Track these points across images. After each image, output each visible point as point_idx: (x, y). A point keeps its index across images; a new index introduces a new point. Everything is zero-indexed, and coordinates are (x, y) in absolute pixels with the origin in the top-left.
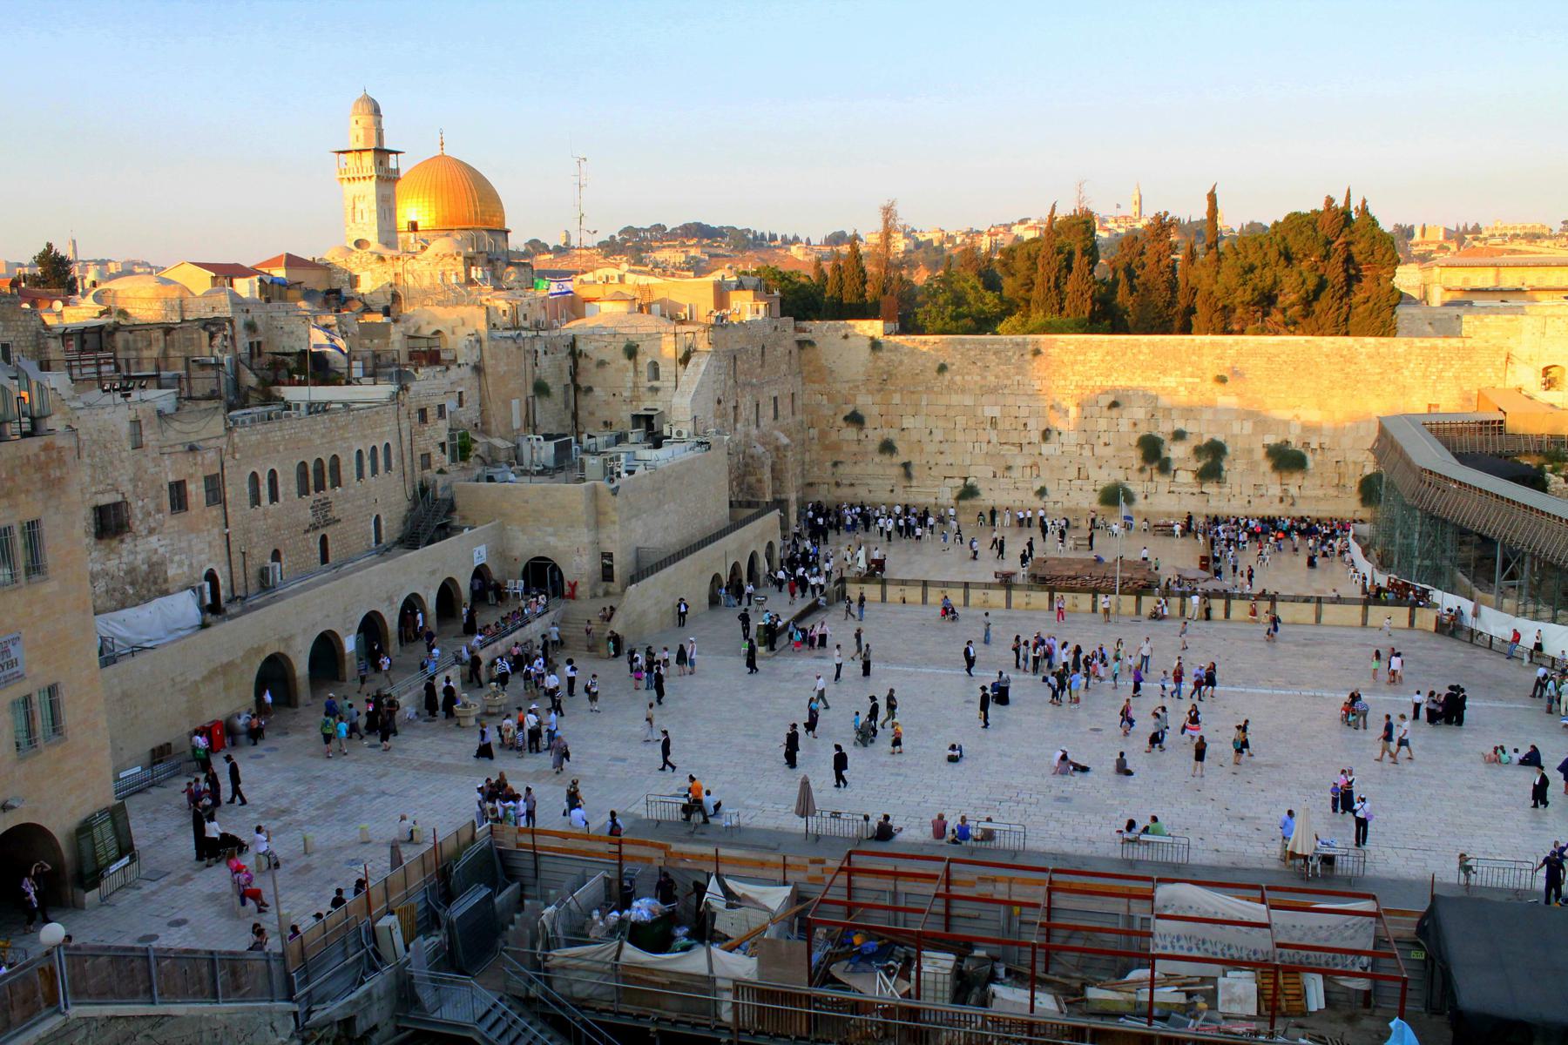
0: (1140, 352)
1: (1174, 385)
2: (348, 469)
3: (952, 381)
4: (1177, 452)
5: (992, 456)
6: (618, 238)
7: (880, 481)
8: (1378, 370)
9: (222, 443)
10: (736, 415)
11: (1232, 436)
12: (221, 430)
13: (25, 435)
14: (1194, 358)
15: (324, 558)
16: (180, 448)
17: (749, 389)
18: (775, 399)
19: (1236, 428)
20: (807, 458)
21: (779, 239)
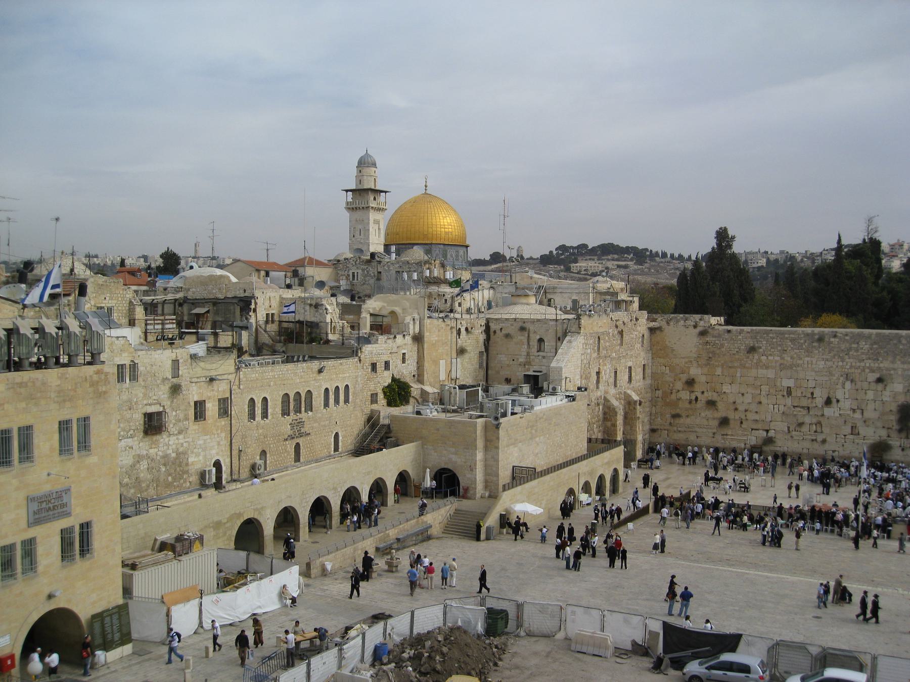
0: (900, 342)
2: (318, 400)
3: (759, 360)
5: (787, 415)
6: (555, 252)
7: (705, 430)
9: (232, 377)
10: (598, 378)
12: (232, 369)
13: (90, 363)
15: (297, 458)
16: (204, 379)
17: (608, 360)
18: (630, 368)
20: (654, 412)
21: (669, 256)
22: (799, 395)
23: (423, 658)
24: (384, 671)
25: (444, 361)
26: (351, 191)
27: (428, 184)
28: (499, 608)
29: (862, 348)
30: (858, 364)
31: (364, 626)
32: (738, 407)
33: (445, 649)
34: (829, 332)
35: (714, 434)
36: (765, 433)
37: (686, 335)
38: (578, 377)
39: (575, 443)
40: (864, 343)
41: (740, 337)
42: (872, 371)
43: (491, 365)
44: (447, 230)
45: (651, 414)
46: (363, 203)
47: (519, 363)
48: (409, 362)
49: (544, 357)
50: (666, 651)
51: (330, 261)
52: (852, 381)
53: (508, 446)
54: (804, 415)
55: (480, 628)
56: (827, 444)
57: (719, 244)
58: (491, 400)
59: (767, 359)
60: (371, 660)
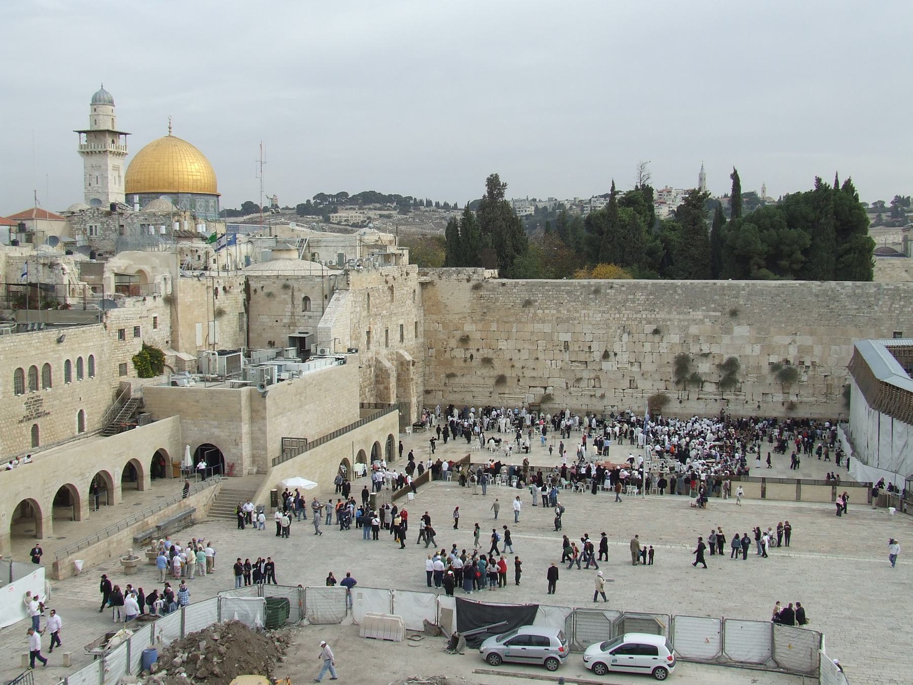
0: (676, 292)
1: (701, 317)
2: (58, 374)
3: (535, 314)
4: (704, 368)
5: (565, 370)
6: (312, 201)
7: (481, 389)
8: (855, 307)
10: (369, 338)
11: (745, 356)
14: (717, 297)
15: (35, 442)
18: (402, 326)
19: (748, 350)
21: (434, 205)
22: (577, 349)
23: (199, 661)
24: (155, 681)
26: (84, 132)
28: (280, 597)
30: (635, 316)
31: (127, 631)
33: (223, 649)
34: (605, 283)
35: (491, 393)
36: (543, 390)
37: (459, 289)
38: (348, 337)
39: (347, 409)
40: (640, 294)
41: (515, 291)
42: (650, 323)
43: (252, 327)
44: (195, 178)
45: (424, 375)
46: (100, 147)
48: (161, 327)
49: (310, 317)
50: (460, 629)
52: (629, 333)
53: (275, 416)
55: (259, 621)
56: (606, 399)
57: (490, 193)
58: (255, 366)
59: (544, 312)
60: (138, 669)
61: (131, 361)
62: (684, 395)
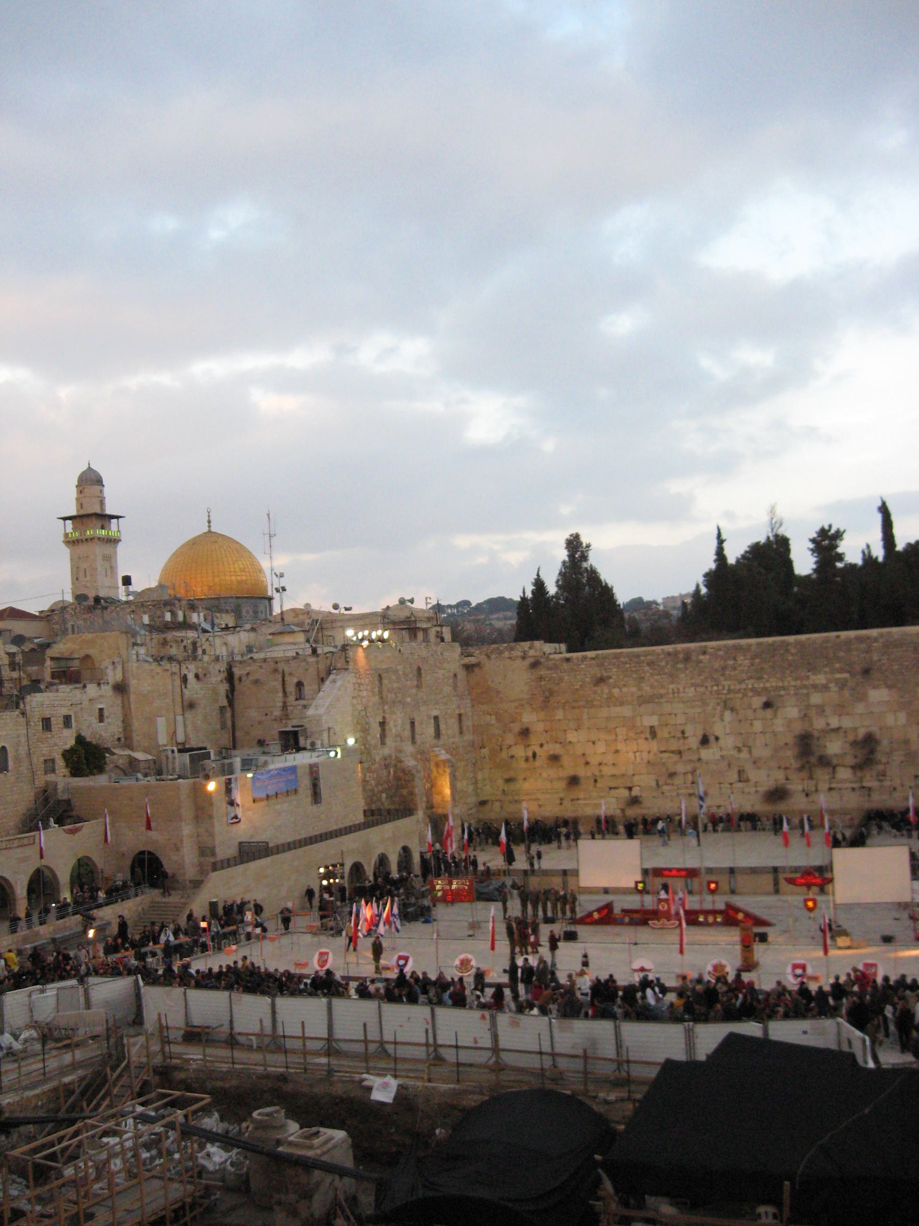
0: (787, 651)
1: (824, 682)
4: (834, 747)
7: (548, 796)
14: (842, 654)
18: (436, 718)
19: (890, 720)
20: (480, 776)
22: (667, 736)
25: (163, 719)
27: (211, 519)
29: (740, 665)
32: (589, 760)
35: (561, 799)
40: (742, 658)
43: (240, 723)
44: (239, 578)
47: (273, 718)
48: (110, 720)
51: (42, 612)
54: (675, 762)
57: (571, 556)
61: (60, 756)
62: (812, 783)
